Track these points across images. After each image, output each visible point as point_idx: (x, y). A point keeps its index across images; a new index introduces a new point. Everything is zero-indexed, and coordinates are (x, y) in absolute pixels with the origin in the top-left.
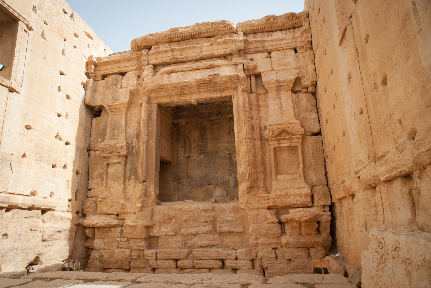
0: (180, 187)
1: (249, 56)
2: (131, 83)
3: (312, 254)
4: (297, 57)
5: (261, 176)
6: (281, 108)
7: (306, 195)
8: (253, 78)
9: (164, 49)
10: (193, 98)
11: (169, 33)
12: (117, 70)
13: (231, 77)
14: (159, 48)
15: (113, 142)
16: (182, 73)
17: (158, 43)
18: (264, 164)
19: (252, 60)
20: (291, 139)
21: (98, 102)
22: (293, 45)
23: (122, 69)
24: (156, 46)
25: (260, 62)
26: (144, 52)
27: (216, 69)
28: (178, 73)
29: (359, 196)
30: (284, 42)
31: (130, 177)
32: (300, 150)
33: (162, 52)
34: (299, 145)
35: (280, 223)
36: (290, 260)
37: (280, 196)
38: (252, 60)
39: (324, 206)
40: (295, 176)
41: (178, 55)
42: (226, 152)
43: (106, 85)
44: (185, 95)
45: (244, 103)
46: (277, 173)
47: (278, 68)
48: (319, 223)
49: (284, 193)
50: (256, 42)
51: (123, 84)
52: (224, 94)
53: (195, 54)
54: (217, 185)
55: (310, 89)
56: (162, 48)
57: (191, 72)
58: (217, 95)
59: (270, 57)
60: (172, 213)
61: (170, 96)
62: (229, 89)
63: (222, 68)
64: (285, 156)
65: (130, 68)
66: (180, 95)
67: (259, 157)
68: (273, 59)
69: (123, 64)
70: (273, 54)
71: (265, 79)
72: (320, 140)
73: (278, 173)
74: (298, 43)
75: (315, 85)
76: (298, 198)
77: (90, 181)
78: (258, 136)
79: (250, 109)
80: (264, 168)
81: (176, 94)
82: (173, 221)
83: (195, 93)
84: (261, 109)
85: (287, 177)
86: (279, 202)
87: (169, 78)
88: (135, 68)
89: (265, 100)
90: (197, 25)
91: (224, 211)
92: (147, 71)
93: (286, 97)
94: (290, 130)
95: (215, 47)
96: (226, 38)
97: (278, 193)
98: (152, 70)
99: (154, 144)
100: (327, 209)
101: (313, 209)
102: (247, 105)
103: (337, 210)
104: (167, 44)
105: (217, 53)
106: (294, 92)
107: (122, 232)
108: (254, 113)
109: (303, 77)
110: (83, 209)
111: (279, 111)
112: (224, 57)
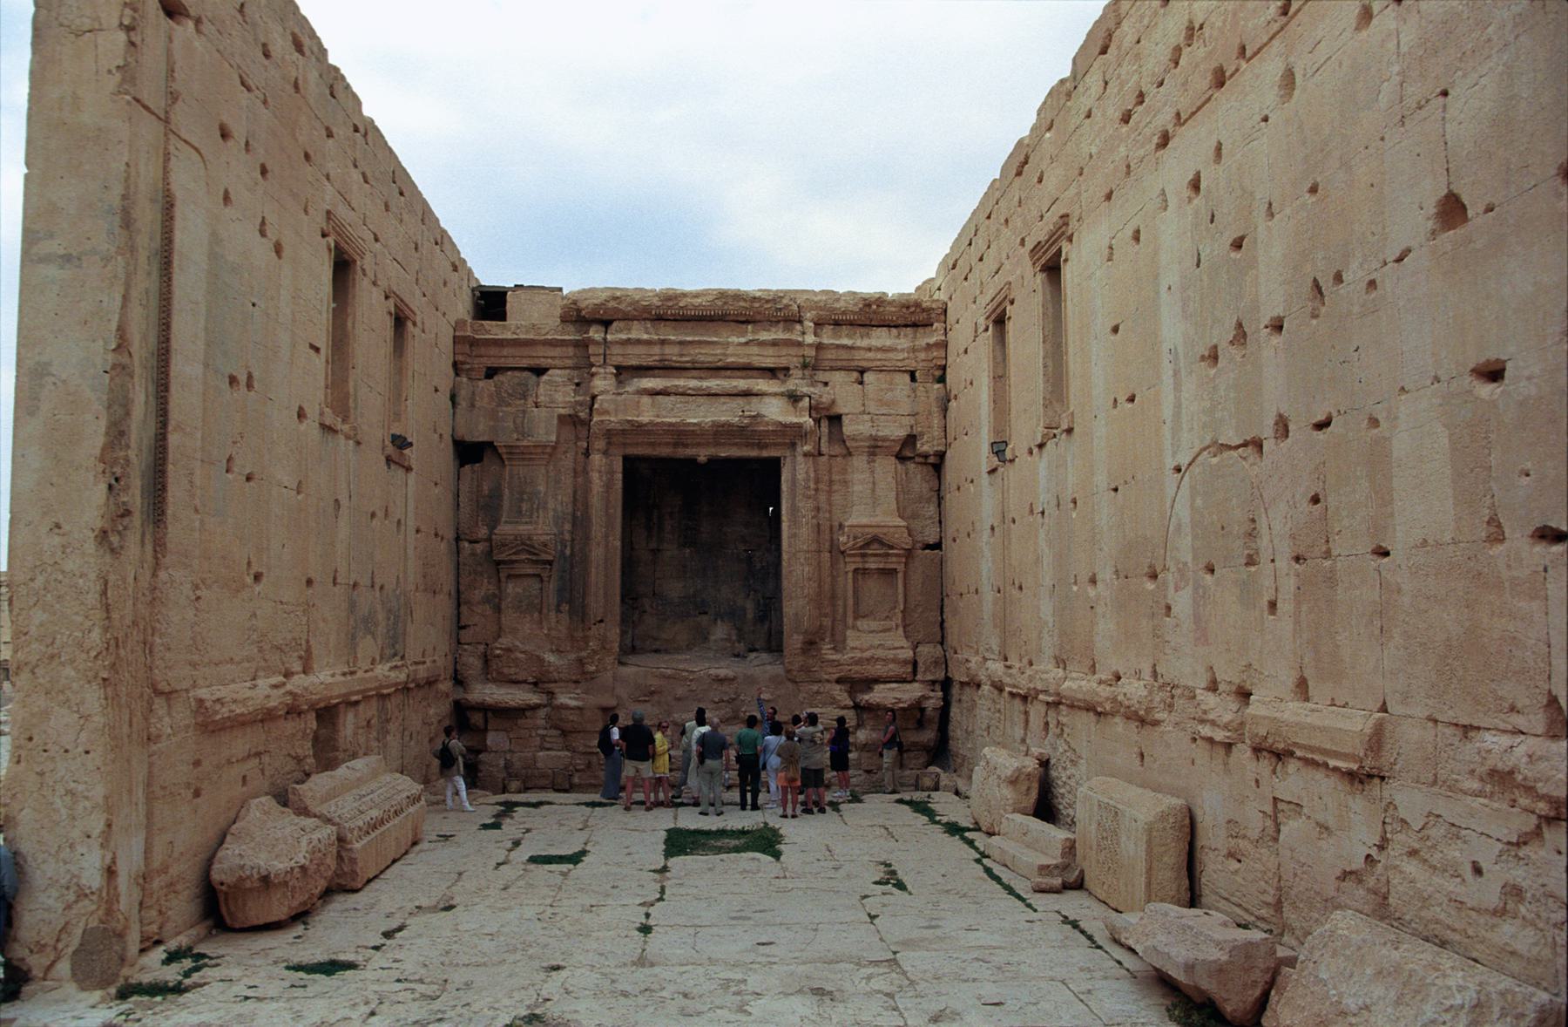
0: (636, 617)
1: (821, 376)
2: (559, 397)
3: (906, 762)
4: (914, 391)
5: (827, 622)
6: (873, 491)
7: (905, 662)
8: (825, 424)
9: (645, 337)
10: (703, 454)
11: (656, 301)
12: (525, 363)
13: (785, 428)
14: (629, 330)
15: (523, 529)
16: (683, 398)
17: (628, 318)
18: (833, 597)
19: (826, 384)
20: (888, 555)
21: (479, 432)
22: (912, 365)
23: (537, 361)
24: (622, 324)
25: (841, 391)
26: (595, 333)
27: (755, 400)
28: (672, 398)
29: (986, 688)
30: (891, 355)
31: (558, 605)
32: (900, 575)
33: (639, 342)
34: (901, 568)
35: (856, 707)
36: (868, 772)
37: (859, 662)
38: (826, 384)
39: (934, 682)
40: (888, 624)
41: (672, 353)
42: (742, 547)
43: (498, 392)
44: (686, 446)
45: (808, 480)
46: (856, 618)
47: (876, 407)
48: (922, 710)
49: (867, 654)
50: (838, 346)
51: (541, 399)
52: (765, 454)
53: (710, 359)
54: (719, 616)
55: (931, 460)
56: (638, 332)
57: (701, 400)
58: (754, 453)
59: (861, 383)
60: (654, 683)
61: (653, 444)
62: (775, 445)
63: (767, 400)
64: (873, 587)
65: (557, 362)
66: (676, 445)
67: (827, 587)
68: (869, 388)
69: (541, 351)
70: (868, 377)
71: (849, 428)
72: (937, 560)
73: (857, 616)
74: (919, 362)
75: (941, 456)
76: (891, 666)
77: (464, 609)
78: (827, 545)
79: (816, 490)
80: (834, 605)
81: (667, 444)
82: (656, 698)
83: (708, 444)
84: (835, 487)
85: (874, 625)
86: (857, 671)
87: (653, 405)
88: (569, 362)
89: (844, 471)
90: (722, 294)
91: (751, 680)
92: (602, 383)
93: (886, 467)
94: (886, 539)
95: (755, 350)
96: (777, 334)
97: (858, 655)
98: (613, 381)
99: (618, 544)
100: (938, 687)
101: (916, 685)
102: (812, 486)
103: (955, 690)
104: (649, 325)
105: (757, 361)
106: (901, 458)
107: (548, 717)
108: (823, 497)
109: (922, 434)
110: (456, 671)
111: (871, 501)
112: (772, 372)
